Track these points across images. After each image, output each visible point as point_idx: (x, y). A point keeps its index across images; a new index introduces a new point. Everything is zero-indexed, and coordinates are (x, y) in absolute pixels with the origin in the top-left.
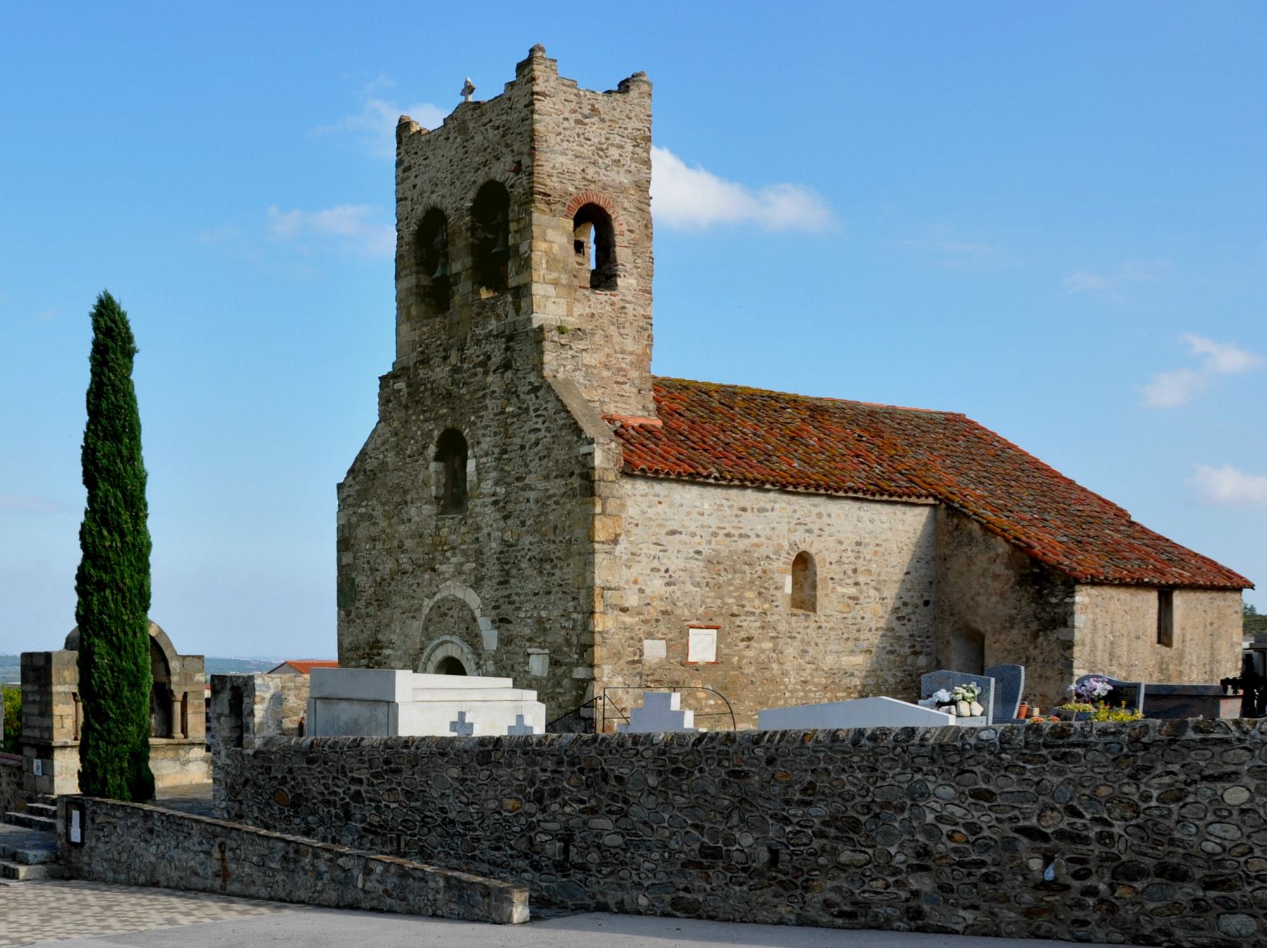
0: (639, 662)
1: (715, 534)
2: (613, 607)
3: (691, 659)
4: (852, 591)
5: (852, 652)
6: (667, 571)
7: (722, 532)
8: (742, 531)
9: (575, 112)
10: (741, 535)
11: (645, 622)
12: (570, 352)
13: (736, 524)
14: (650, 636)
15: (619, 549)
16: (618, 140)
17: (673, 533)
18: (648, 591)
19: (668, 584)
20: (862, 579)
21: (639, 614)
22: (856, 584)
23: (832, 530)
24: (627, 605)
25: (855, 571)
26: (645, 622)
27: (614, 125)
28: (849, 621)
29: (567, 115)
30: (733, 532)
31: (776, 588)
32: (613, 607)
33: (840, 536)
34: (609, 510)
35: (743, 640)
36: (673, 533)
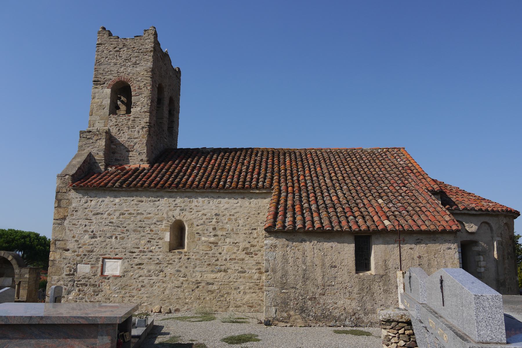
0: (73, 274)
1: (123, 214)
2: (59, 248)
3: (106, 273)
4: (212, 239)
5: (212, 271)
6: (92, 232)
7: (127, 213)
8: (139, 212)
9: (115, 48)
10: (138, 214)
11: (78, 256)
12: (92, 141)
13: (135, 208)
14: (81, 262)
15: (66, 222)
16: (136, 54)
17: (97, 214)
18: (82, 241)
19: (92, 238)
20: (219, 233)
21: (74, 252)
22: (215, 236)
23: (199, 209)
24: (68, 248)
25: (214, 229)
26: (78, 256)
27: (134, 49)
28: (211, 255)
29: (111, 50)
30: (133, 212)
31: (159, 239)
32: (59, 248)
33: (204, 212)
34: (62, 205)
35: (137, 265)
36: (97, 214)
